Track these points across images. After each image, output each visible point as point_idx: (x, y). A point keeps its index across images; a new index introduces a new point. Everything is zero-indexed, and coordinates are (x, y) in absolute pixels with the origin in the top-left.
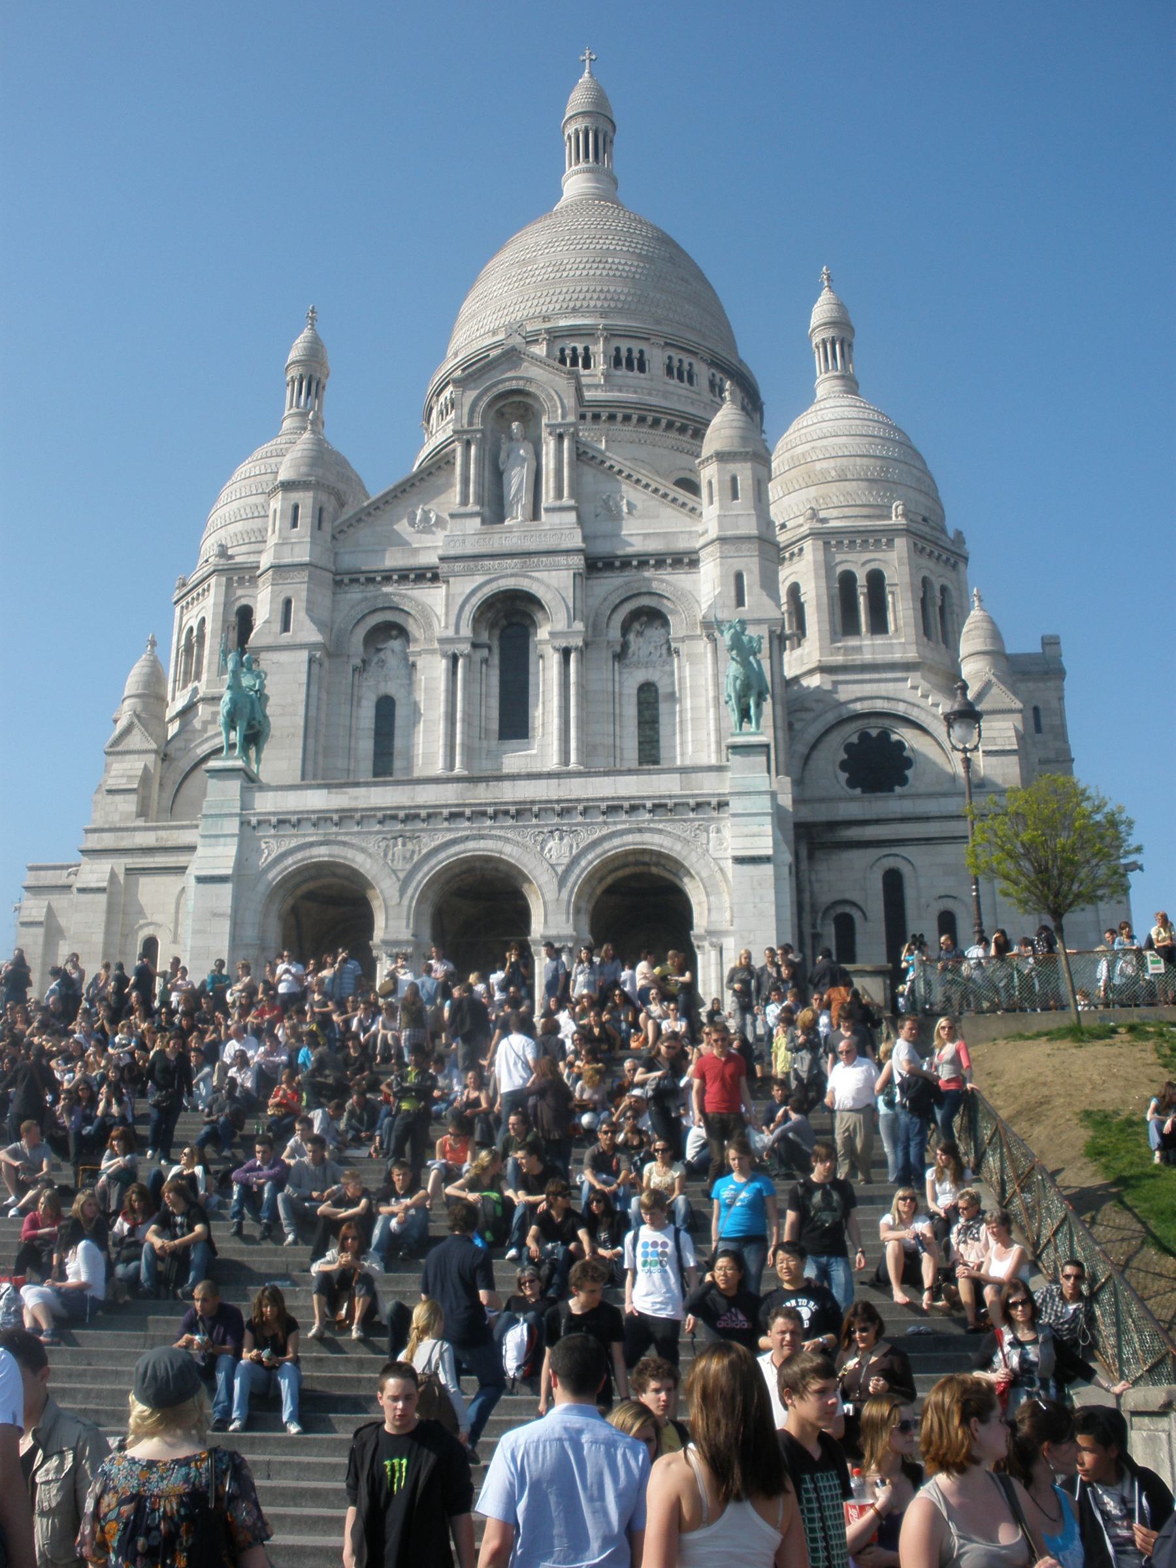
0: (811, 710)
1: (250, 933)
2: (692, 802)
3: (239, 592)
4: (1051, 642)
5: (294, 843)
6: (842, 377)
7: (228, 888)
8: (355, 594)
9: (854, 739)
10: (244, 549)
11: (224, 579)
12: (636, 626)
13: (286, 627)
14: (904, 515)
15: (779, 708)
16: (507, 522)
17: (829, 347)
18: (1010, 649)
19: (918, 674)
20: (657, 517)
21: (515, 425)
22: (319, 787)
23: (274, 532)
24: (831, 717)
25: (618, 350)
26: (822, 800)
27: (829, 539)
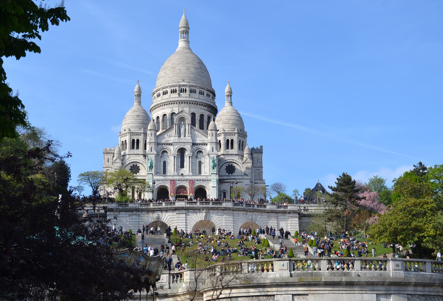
0: (221, 161)
3: (132, 137)
4: (261, 147)
6: (229, 102)
8: (160, 146)
9: (227, 165)
10: (132, 129)
12: (199, 153)
13: (151, 151)
14: (237, 131)
15: (217, 166)
16: (181, 137)
19: (237, 156)
21: (182, 122)
24: (224, 162)
25: (191, 89)
26: (222, 176)
27: (225, 134)
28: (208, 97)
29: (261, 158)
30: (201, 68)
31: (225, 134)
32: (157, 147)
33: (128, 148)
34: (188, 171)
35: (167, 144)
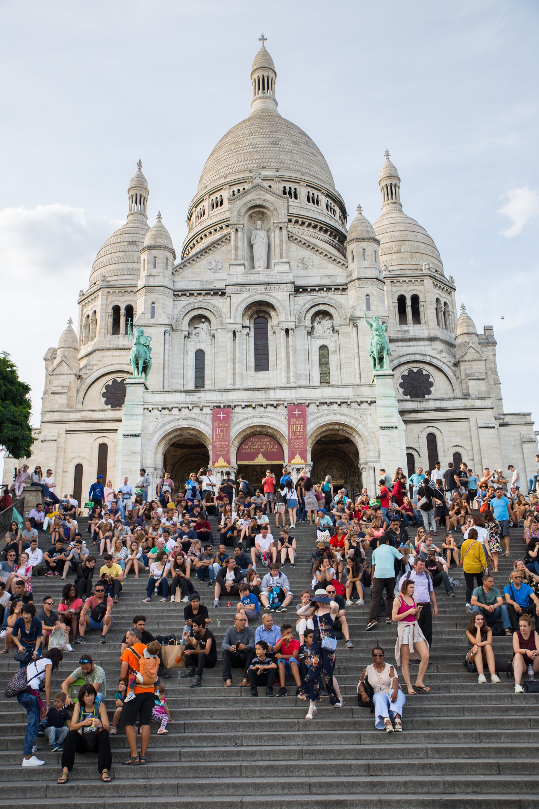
1: (149, 463)
2: (359, 401)
3: (114, 299)
5: (170, 418)
6: (396, 203)
7: (139, 439)
8: (184, 301)
9: (406, 373)
11: (105, 292)
12: (318, 319)
13: (153, 316)
14: (429, 269)
17: (389, 188)
18: (478, 333)
20: (327, 268)
22: (181, 392)
23: (144, 270)
25: (285, 188)
27: (394, 279)
28: (329, 213)
29: (491, 358)
30: (307, 144)
31: (392, 279)
32: (171, 304)
33: (100, 333)
34: (284, 380)
35: (209, 294)
